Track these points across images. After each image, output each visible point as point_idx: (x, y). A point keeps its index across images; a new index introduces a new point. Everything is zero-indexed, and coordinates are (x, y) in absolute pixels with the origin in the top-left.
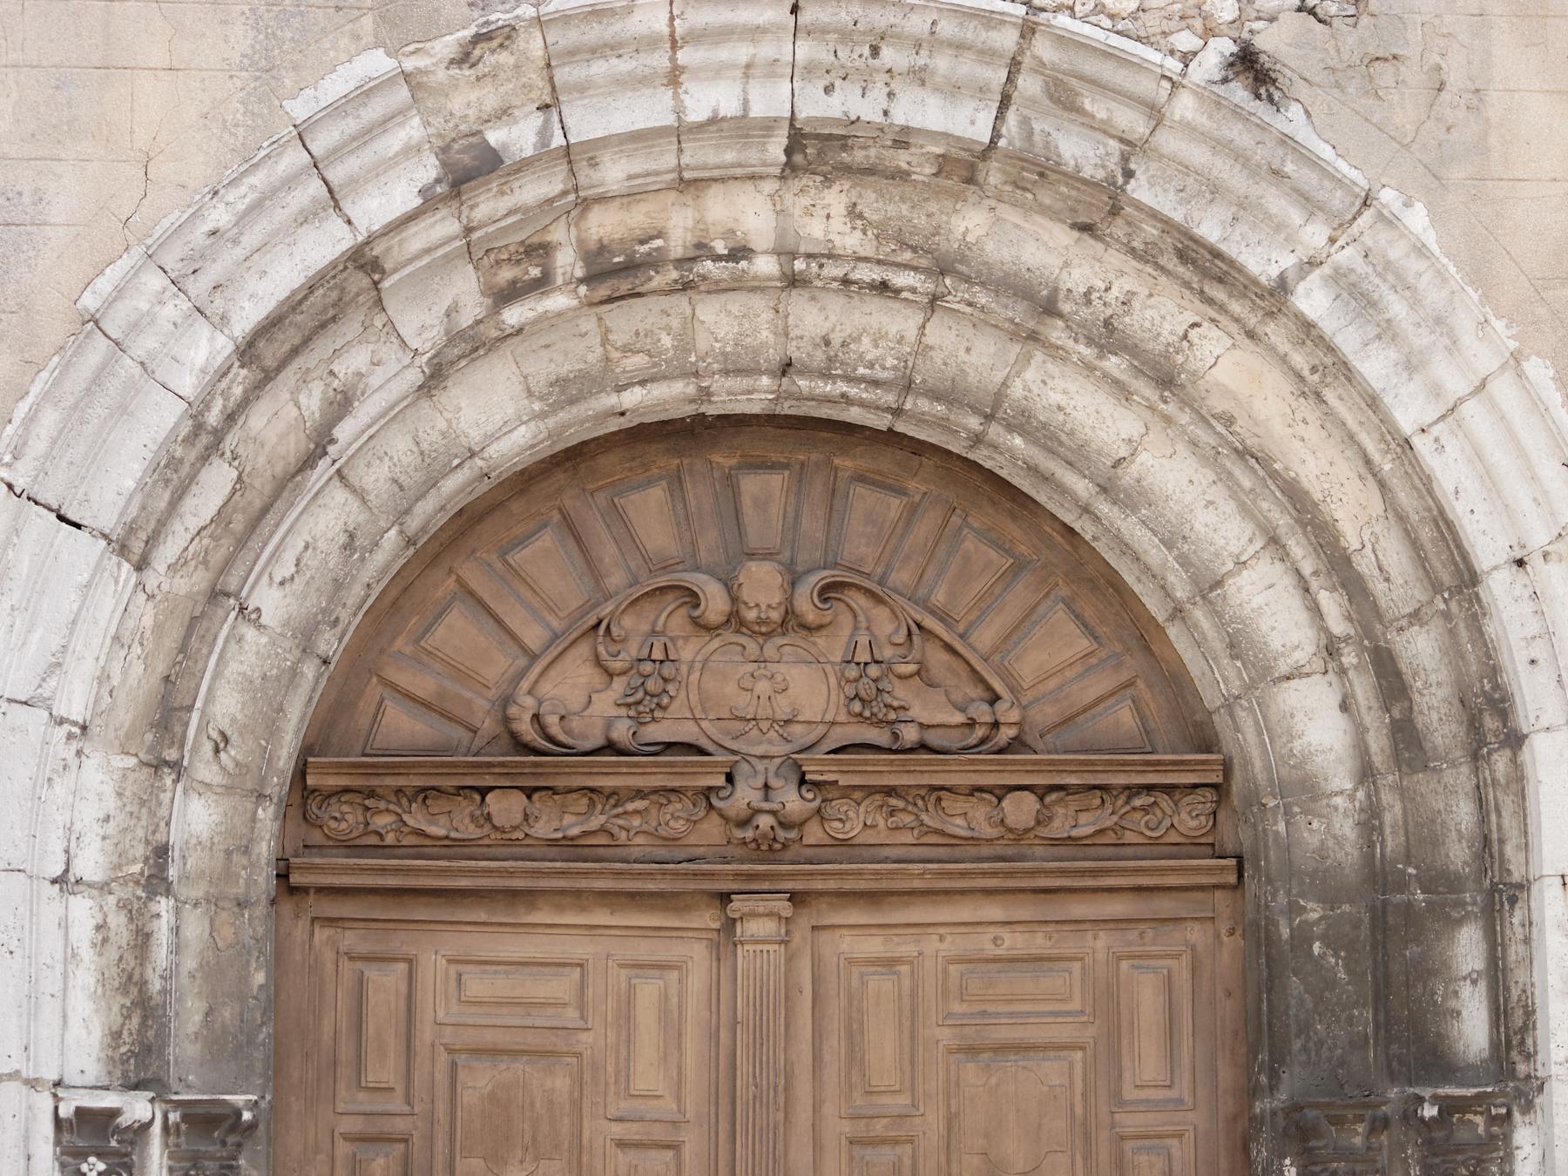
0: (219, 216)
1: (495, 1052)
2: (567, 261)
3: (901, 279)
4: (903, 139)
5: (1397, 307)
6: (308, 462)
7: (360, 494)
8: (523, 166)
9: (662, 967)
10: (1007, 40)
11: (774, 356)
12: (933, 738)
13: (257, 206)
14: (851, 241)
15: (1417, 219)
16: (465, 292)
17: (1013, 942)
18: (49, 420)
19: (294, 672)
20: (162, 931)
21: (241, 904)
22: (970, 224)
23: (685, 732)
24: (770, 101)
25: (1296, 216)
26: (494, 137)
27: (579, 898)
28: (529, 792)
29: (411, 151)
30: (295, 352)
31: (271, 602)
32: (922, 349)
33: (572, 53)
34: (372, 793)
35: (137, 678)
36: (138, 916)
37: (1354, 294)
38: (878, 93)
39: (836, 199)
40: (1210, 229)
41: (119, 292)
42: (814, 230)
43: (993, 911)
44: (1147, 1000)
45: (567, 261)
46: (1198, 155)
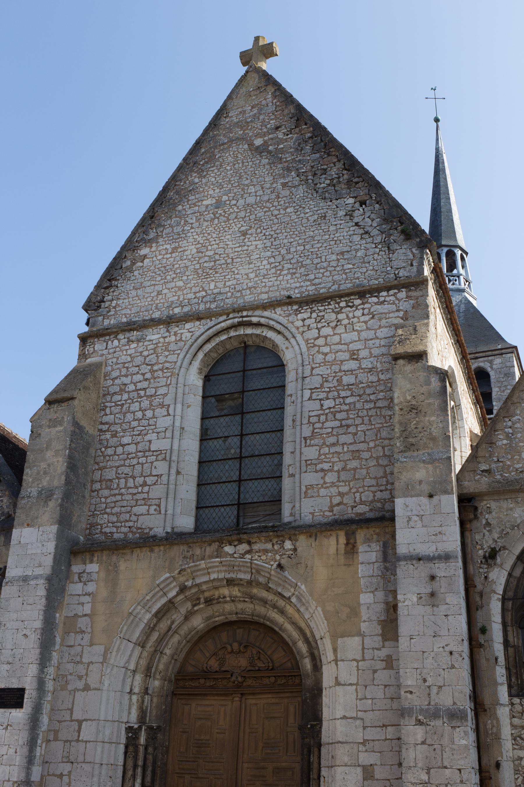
0: (148, 598)
1: (200, 719)
2: (202, 600)
3: (247, 600)
4: (241, 580)
5: (304, 600)
6: (168, 631)
7: (180, 635)
8: (191, 588)
9: (225, 705)
10: (249, 565)
11: (235, 612)
12: (261, 669)
13: (154, 596)
14: (239, 594)
15: (303, 587)
16: (189, 605)
17: (273, 701)
18: (125, 628)
19: (171, 662)
20: (146, 700)
21: (162, 696)
22: (255, 591)
23: (227, 669)
24: (221, 576)
25: (290, 588)
26: (186, 584)
27: (213, 695)
28: (205, 679)
29: (175, 587)
30: (163, 616)
31: (168, 651)
32: (255, 610)
33: (194, 571)
34: (185, 679)
35: (143, 663)
37: (299, 599)
38: (235, 574)
39: (236, 589)
40: (280, 590)
41: (134, 609)
42: (234, 593)
43: (270, 696)
44: (292, 709)
45: (202, 600)
46: (276, 579)
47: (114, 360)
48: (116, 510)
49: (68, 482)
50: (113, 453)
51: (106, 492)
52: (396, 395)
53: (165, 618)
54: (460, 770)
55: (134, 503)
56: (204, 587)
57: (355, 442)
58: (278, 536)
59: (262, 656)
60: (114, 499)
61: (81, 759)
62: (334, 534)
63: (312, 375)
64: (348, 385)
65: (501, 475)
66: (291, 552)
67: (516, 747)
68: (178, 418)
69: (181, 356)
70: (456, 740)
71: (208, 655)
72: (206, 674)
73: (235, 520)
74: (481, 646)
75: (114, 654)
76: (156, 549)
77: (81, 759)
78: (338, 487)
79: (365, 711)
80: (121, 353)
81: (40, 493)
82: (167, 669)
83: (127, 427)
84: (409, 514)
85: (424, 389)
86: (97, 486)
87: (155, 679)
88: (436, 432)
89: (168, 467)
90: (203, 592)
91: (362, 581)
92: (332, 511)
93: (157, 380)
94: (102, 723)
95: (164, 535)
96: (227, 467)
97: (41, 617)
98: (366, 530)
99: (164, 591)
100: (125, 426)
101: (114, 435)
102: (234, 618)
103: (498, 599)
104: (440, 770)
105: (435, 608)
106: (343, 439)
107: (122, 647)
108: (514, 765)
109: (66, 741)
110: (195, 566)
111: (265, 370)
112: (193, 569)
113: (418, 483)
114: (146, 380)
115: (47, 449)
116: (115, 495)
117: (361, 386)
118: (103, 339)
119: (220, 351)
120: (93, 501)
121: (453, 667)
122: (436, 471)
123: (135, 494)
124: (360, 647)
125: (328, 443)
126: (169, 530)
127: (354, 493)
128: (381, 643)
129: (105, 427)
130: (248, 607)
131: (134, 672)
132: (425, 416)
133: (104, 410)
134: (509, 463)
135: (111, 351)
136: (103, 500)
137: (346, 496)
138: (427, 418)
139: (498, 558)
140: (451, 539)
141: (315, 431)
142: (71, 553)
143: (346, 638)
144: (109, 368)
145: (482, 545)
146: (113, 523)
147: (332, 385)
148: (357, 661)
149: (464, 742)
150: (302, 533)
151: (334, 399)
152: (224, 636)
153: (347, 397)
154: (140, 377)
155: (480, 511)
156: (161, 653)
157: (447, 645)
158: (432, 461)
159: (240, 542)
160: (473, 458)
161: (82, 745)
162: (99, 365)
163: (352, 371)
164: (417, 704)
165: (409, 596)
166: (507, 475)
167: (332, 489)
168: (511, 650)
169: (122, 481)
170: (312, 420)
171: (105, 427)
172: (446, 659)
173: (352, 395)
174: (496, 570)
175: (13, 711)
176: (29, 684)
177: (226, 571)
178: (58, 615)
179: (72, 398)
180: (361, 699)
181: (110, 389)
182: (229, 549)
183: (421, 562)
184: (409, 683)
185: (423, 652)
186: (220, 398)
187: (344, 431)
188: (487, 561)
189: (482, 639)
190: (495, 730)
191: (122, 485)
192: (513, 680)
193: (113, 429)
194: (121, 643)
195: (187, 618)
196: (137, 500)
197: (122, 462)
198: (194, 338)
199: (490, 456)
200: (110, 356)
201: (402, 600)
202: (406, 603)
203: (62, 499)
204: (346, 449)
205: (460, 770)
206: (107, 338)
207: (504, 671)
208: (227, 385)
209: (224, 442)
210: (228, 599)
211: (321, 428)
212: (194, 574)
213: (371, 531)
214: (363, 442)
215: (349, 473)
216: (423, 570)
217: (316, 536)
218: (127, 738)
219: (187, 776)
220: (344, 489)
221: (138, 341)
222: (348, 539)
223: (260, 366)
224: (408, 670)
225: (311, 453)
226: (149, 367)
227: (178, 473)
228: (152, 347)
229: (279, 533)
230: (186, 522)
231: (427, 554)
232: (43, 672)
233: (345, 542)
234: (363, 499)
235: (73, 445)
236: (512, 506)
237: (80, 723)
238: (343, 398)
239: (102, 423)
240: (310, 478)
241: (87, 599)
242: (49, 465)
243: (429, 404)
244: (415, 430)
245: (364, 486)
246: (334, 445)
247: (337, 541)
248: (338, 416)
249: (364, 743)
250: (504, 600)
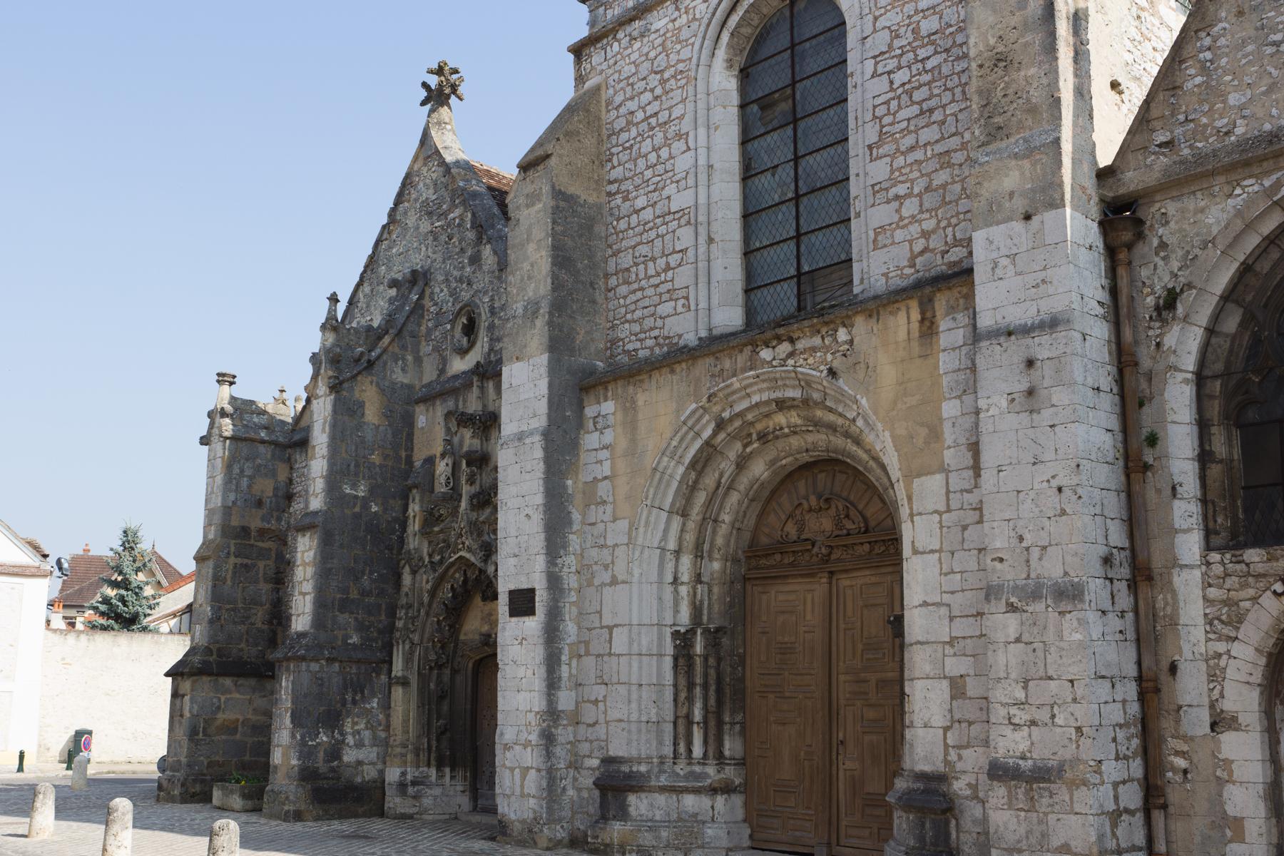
0: (674, 443)
1: (783, 612)
2: (754, 436)
4: (794, 399)
6: (717, 488)
10: (793, 375)
13: (682, 440)
14: (799, 422)
16: (738, 446)
17: (873, 579)
18: (652, 491)
20: (699, 591)
22: (819, 413)
24: (765, 397)
29: (708, 422)
31: (726, 517)
35: (690, 538)
36: (695, 589)
39: (794, 413)
40: (840, 410)
41: (659, 463)
43: (868, 572)
47: (616, 76)
48: (638, 314)
49: (557, 285)
50: (626, 226)
51: (623, 290)
52: (972, 41)
53: (708, 469)
54: (1071, 681)
55: (656, 299)
56: (750, 417)
57: (943, 138)
58: (826, 323)
59: (851, 513)
60: (633, 298)
61: (615, 680)
62: (902, 306)
63: (875, 31)
64: (929, 36)
65: (1191, 147)
66: (847, 347)
67: (1212, 636)
68: (702, 152)
69: (697, 47)
70: (1064, 633)
71: (783, 517)
72: (781, 546)
73: (795, 304)
74: (1146, 467)
75: (641, 530)
76: (678, 368)
77: (615, 680)
78: (920, 221)
79: (952, 593)
80: (622, 62)
81: (525, 308)
82: (728, 544)
83: (640, 182)
84: (995, 255)
85: (1015, 20)
86: (613, 281)
87: (711, 559)
88: (1037, 96)
89: (693, 234)
90: (752, 424)
91: (945, 381)
92: (913, 266)
93: (671, 94)
94: (635, 629)
95: (697, 343)
96: (780, 217)
97: (542, 489)
98: (947, 293)
99: (696, 429)
100: (638, 181)
101: (626, 199)
102: (805, 458)
103: (1186, 381)
104: (1042, 682)
105: (1035, 416)
106: (929, 134)
107: (652, 519)
108: (1208, 666)
109: (598, 656)
110: (727, 386)
111: (822, 38)
112: (726, 392)
113: (1007, 197)
114: (656, 98)
115: (528, 240)
116: (634, 292)
117: (947, 32)
118: (599, 45)
119: (756, 22)
120: (611, 306)
121: (1063, 513)
122: (1035, 170)
123: (657, 286)
124: (944, 491)
125: (903, 148)
126: (703, 334)
127: (944, 228)
128: (973, 481)
129: (613, 188)
130: (820, 438)
131: (678, 553)
132: (1019, 69)
133: (610, 160)
134: (1204, 120)
135: (612, 62)
136: (622, 301)
137: (933, 237)
138: (1022, 73)
139: (1179, 305)
140: (1061, 290)
141: (884, 130)
142: (581, 389)
143: (923, 478)
144: (611, 91)
145: (1152, 287)
146: (636, 335)
147: (904, 42)
148: (940, 513)
149: (1078, 636)
150: (857, 313)
151: (909, 67)
152: (802, 486)
153: (928, 58)
154: (648, 96)
155: (1148, 223)
156: (715, 521)
157: (1053, 477)
158: (1029, 152)
159: (780, 339)
160: (1143, 121)
161: (614, 659)
162: (597, 89)
163: (933, 7)
164: (1009, 577)
165: (995, 399)
166: (1200, 145)
167: (911, 228)
168: (1215, 470)
169: (642, 267)
170: (879, 112)
171: (613, 188)
172: (1051, 501)
173: (936, 53)
174: (1176, 329)
175: (526, 619)
176: (539, 583)
177: (769, 389)
178: (569, 482)
179: (548, 156)
180: (946, 574)
181: (615, 125)
182: (765, 354)
183: (1013, 337)
184: (998, 545)
185: (1019, 492)
186: (766, 103)
187: (926, 120)
188: (1160, 315)
189: (1149, 456)
190: (1169, 610)
191: (642, 275)
192: (1219, 520)
193: (623, 188)
194: (650, 513)
195: (741, 464)
196: (661, 294)
197: (638, 239)
198: (711, 10)
199: (1173, 115)
200: (611, 71)
201: (985, 407)
202: (990, 413)
203: (550, 313)
204: (929, 153)
205: (1071, 681)
206: (605, 41)
207: (1195, 508)
208: (773, 78)
209: (773, 175)
210: (786, 430)
211: (892, 124)
212: (730, 399)
213: (955, 292)
214: (954, 135)
215: (935, 194)
216: (1016, 350)
217: (878, 314)
218: (675, 647)
219: (771, 696)
220: (929, 225)
221: (642, 36)
222: (923, 313)
223: (815, 32)
224: (995, 524)
225: (879, 170)
226: (658, 77)
227: (710, 240)
228: (659, 41)
229: (826, 318)
230: (730, 317)
231: (1023, 322)
232: (556, 565)
233: (919, 317)
234: (959, 236)
235: (559, 228)
236: (1203, 204)
237: (610, 629)
238: (923, 60)
239: (610, 182)
240: (881, 214)
241: (604, 454)
242: (532, 265)
243: (1026, 45)
244: (1003, 100)
245: (958, 213)
246: (912, 149)
247: (908, 318)
248: (917, 96)
249: (952, 641)
250: (1200, 378)
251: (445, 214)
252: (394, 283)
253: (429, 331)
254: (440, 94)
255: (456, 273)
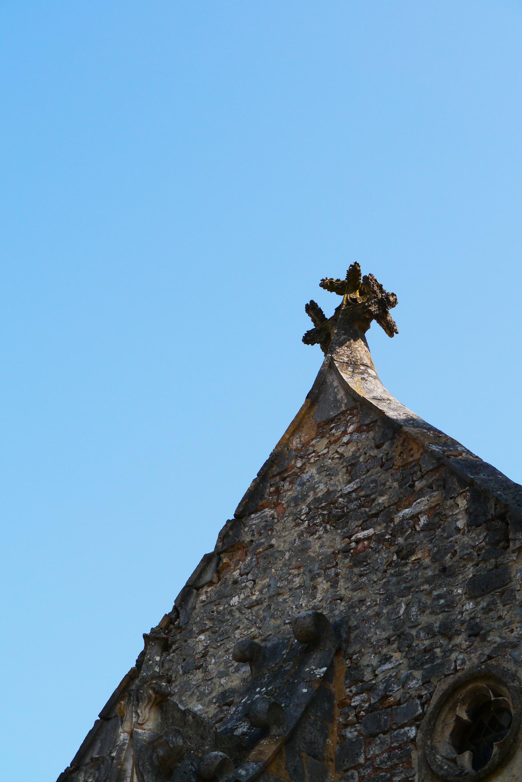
251: (387, 514)
252: (250, 654)
253: (348, 750)
254: (357, 307)
255: (425, 619)
